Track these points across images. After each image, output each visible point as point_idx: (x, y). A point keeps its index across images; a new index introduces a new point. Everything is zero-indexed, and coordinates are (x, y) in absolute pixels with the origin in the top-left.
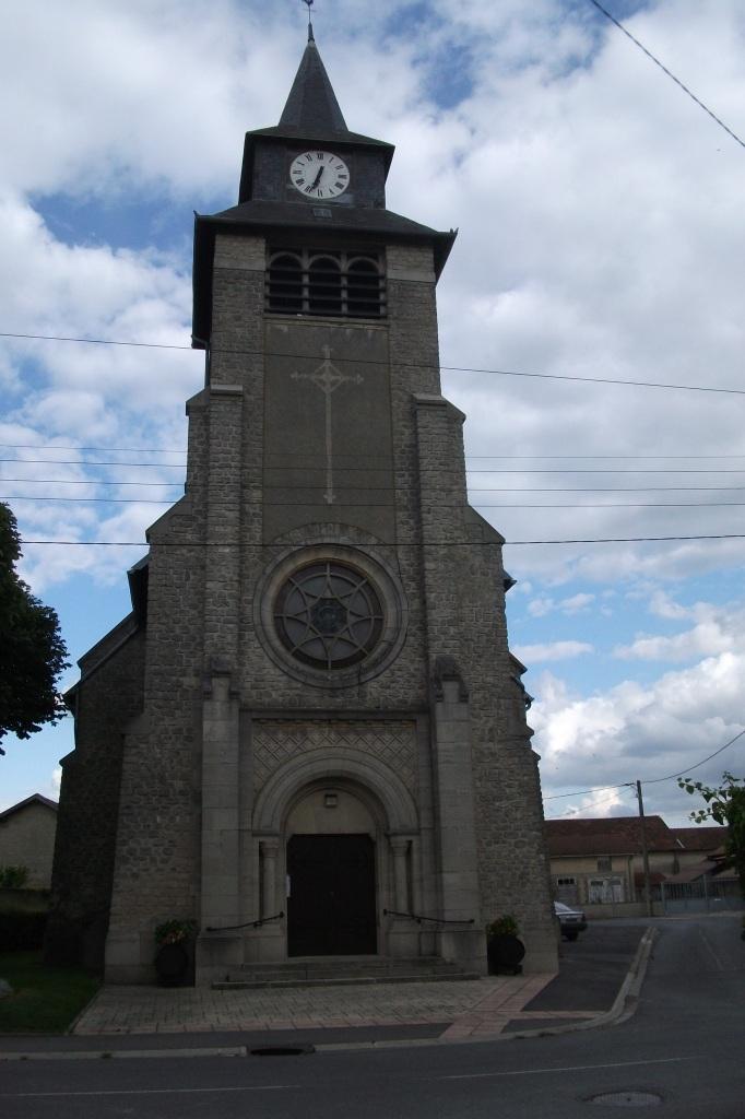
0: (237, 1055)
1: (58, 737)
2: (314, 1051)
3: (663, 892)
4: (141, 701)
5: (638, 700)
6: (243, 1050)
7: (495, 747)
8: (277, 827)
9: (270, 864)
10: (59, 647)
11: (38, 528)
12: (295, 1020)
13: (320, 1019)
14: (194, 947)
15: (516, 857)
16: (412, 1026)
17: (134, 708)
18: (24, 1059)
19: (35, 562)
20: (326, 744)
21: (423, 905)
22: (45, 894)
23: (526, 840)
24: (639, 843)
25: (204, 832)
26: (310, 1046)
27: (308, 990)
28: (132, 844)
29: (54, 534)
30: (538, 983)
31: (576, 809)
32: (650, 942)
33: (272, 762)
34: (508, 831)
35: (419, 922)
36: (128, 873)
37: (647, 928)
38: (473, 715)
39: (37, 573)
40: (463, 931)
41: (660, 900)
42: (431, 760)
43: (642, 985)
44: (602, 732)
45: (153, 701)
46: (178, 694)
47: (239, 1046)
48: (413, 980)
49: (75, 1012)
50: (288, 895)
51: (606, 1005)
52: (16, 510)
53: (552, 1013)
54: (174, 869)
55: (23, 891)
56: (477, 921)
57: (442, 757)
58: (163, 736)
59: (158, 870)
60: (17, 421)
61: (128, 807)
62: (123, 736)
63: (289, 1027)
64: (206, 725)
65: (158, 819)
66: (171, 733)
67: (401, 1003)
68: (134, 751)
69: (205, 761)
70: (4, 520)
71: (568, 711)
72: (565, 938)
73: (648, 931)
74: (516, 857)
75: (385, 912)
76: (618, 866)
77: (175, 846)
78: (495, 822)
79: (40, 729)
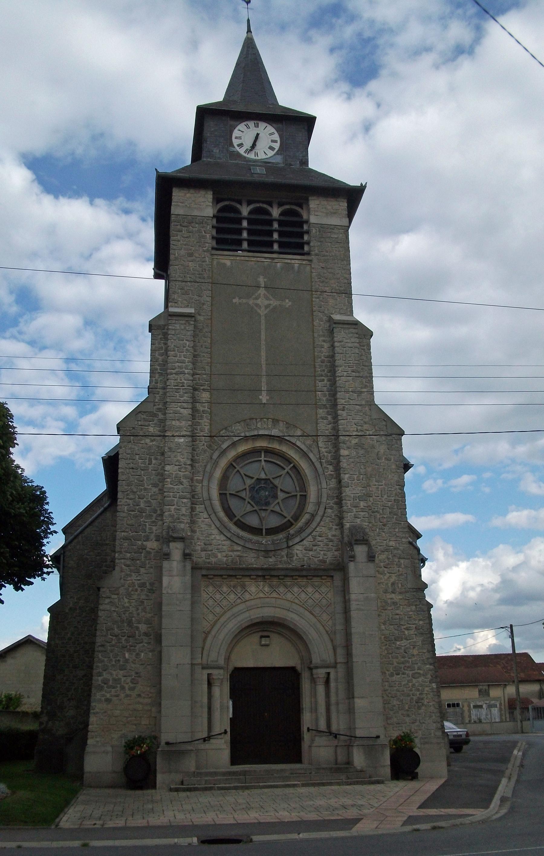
0: (189, 844)
1: (47, 589)
2: (251, 841)
3: (531, 714)
4: (113, 561)
5: (511, 560)
6: (195, 840)
7: (396, 597)
8: (221, 662)
9: (216, 691)
10: (47, 518)
11: (31, 423)
12: (236, 816)
13: (257, 815)
14: (155, 758)
15: (414, 685)
16: (329, 821)
17: (106, 566)
18: (19, 847)
19: (28, 449)
20: (262, 595)
21: (339, 724)
22: (36, 716)
23: (421, 672)
24: (512, 674)
25: (163, 665)
26: (249, 837)
27: (247, 792)
28: (105, 675)
29: (43, 427)
30: (432, 787)
31: (461, 647)
32: (520, 753)
33: (218, 610)
34: (407, 665)
35: (336, 737)
36: (103, 698)
37: (518, 742)
38: (378, 571)
39: (29, 459)
40: (371, 745)
41: (529, 719)
42: (345, 608)
43: (514, 788)
44: (482, 585)
45: (123, 561)
46: (143, 555)
47: (191, 837)
48: (331, 784)
49: (60, 808)
50: (231, 716)
51: (486, 803)
52: (13, 408)
53: (442, 810)
54: (139, 696)
55: (18, 712)
56: (382, 737)
57: (353, 605)
58: (130, 589)
59: (127, 696)
60: (13, 337)
61: (102, 646)
62: (99, 589)
63: (232, 822)
64: (165, 580)
65: (127, 655)
66: (137, 587)
67: (321, 802)
68: (107, 601)
69: (164, 608)
70: (3, 416)
71: (455, 568)
72: (452, 750)
73: (519, 744)
74: (414, 685)
75: (308, 730)
76: (495, 692)
77: (140, 677)
78: (397, 658)
79: (32, 583)
